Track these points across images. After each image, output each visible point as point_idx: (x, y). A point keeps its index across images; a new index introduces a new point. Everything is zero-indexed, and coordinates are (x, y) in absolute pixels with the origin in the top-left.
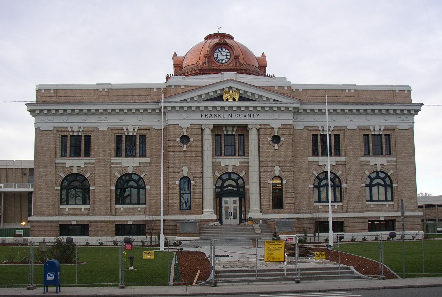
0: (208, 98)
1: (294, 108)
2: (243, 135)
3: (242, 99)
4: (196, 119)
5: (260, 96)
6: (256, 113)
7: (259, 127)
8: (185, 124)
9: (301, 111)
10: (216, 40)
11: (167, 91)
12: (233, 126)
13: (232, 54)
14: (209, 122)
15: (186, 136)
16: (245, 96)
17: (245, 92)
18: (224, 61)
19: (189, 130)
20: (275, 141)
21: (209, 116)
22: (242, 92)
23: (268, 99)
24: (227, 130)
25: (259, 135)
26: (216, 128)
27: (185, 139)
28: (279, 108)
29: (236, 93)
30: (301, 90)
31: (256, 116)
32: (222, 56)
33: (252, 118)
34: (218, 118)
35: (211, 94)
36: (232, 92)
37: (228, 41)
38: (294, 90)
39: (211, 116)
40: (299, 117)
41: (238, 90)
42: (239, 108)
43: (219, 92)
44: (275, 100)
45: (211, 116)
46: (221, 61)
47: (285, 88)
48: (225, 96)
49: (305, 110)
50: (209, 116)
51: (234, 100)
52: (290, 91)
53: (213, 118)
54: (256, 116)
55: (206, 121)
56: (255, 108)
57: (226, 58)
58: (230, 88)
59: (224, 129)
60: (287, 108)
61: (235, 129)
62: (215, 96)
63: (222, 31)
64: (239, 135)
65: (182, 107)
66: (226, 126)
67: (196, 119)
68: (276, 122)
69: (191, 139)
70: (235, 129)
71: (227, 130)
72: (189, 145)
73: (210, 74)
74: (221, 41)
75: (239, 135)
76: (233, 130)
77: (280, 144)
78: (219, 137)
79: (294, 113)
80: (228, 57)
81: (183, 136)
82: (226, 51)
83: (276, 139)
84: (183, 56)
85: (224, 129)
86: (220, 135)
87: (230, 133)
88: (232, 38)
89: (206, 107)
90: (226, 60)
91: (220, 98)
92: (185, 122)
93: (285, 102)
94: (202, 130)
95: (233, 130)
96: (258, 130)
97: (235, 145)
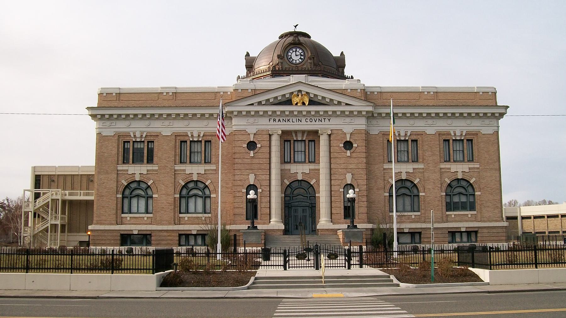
0: (277, 102)
1: (367, 112)
2: (314, 141)
3: (312, 102)
4: (264, 124)
5: (331, 100)
6: (326, 118)
7: (329, 132)
8: (252, 130)
9: (376, 115)
10: (290, 39)
11: (240, 95)
12: (303, 132)
13: (306, 54)
14: (278, 127)
15: (253, 142)
16: (316, 100)
17: (316, 96)
18: (298, 62)
19: (256, 136)
20: (347, 147)
21: (277, 120)
22: (312, 96)
23: (339, 103)
24: (296, 136)
25: (330, 141)
26: (284, 132)
27: (252, 145)
28: (351, 112)
29: (306, 97)
30: (376, 93)
31: (327, 120)
32: (296, 56)
33: (323, 122)
34: (287, 123)
35: (279, 98)
36: (302, 95)
37: (302, 39)
38: (368, 93)
39: (279, 120)
40: (374, 122)
41: (308, 93)
42: (309, 112)
43: (287, 96)
44: (347, 104)
45: (274, 120)
46: (294, 62)
47: (359, 91)
48: (295, 100)
49: (380, 114)
50: (277, 120)
51: (304, 104)
52: (367, 95)
53: (282, 123)
54: (327, 120)
55: (273, 127)
56: (326, 112)
57: (300, 58)
58: (300, 91)
59: (294, 135)
60: (359, 112)
61: (305, 135)
62: (284, 99)
63: (298, 30)
64: (309, 141)
65: (249, 112)
66: (296, 132)
67: (264, 124)
68: (348, 127)
69: (259, 146)
70: (305, 135)
71: (296, 136)
72: (256, 151)
73: (283, 76)
74: (296, 39)
75: (309, 141)
76: (303, 136)
77: (352, 151)
78: (289, 143)
79: (368, 118)
80: (302, 57)
81: (251, 142)
82: (300, 51)
83: (348, 145)
84: (257, 56)
85: (294, 135)
86: (290, 141)
87: (300, 139)
88: (309, 37)
89: (274, 112)
90: (300, 60)
91: (288, 102)
92: (251, 127)
93: (360, 106)
94: (270, 135)
95: (303, 136)
96: (330, 135)
97: (305, 152)
